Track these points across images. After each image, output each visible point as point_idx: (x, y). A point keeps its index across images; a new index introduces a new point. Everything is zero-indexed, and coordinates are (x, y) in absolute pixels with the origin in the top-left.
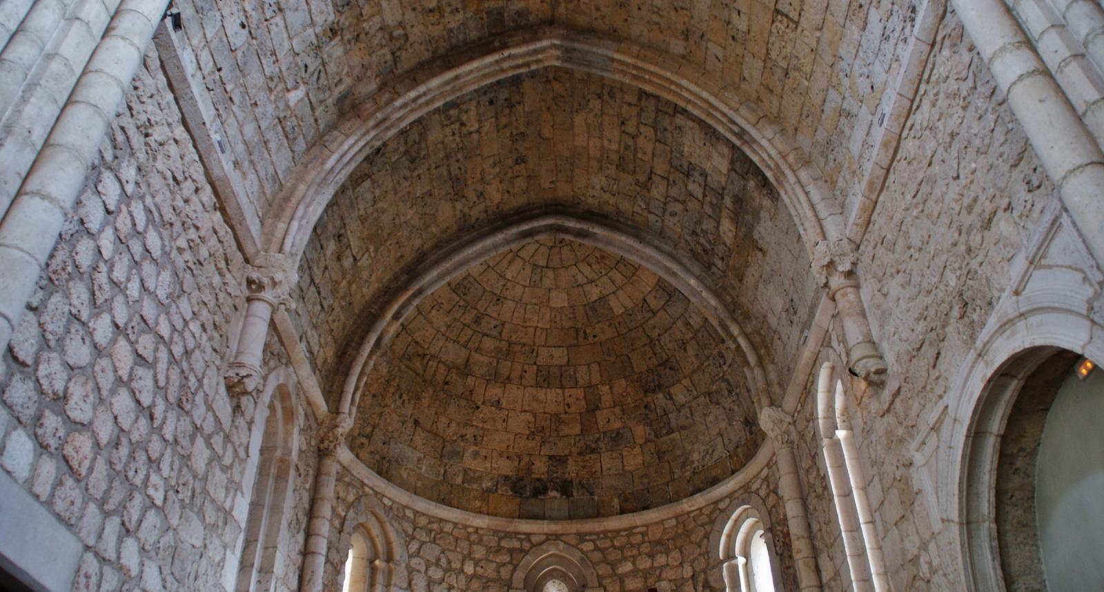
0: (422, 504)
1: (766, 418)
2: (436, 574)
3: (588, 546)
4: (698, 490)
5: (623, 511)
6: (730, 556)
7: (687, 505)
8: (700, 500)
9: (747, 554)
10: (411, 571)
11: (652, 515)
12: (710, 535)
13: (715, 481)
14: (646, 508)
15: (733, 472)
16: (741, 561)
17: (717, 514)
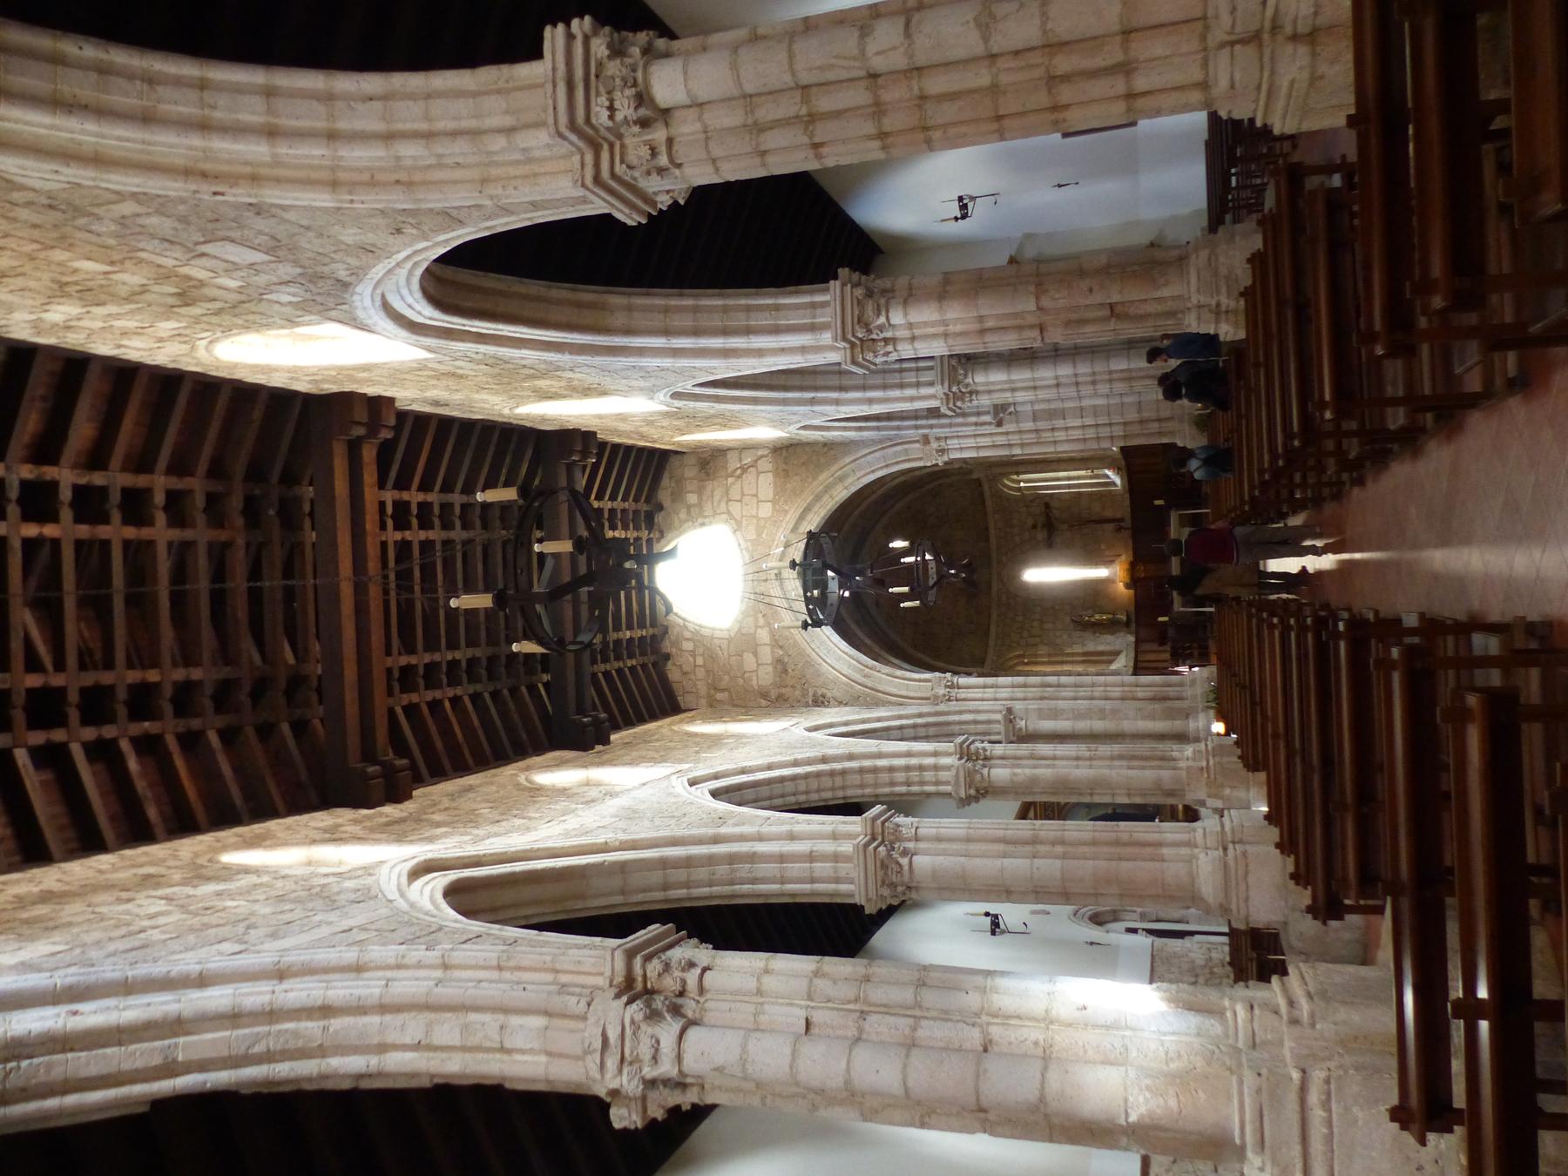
0: (992, 642)
1: (975, 476)
2: (1025, 634)
3: (1004, 559)
4: (984, 502)
5: (987, 539)
6: (1020, 489)
7: (989, 509)
8: (989, 503)
9: (1019, 482)
10: (1027, 645)
11: (991, 525)
12: (1009, 498)
13: (982, 494)
14: (987, 529)
15: (980, 485)
16: (1022, 484)
17: (999, 496)
